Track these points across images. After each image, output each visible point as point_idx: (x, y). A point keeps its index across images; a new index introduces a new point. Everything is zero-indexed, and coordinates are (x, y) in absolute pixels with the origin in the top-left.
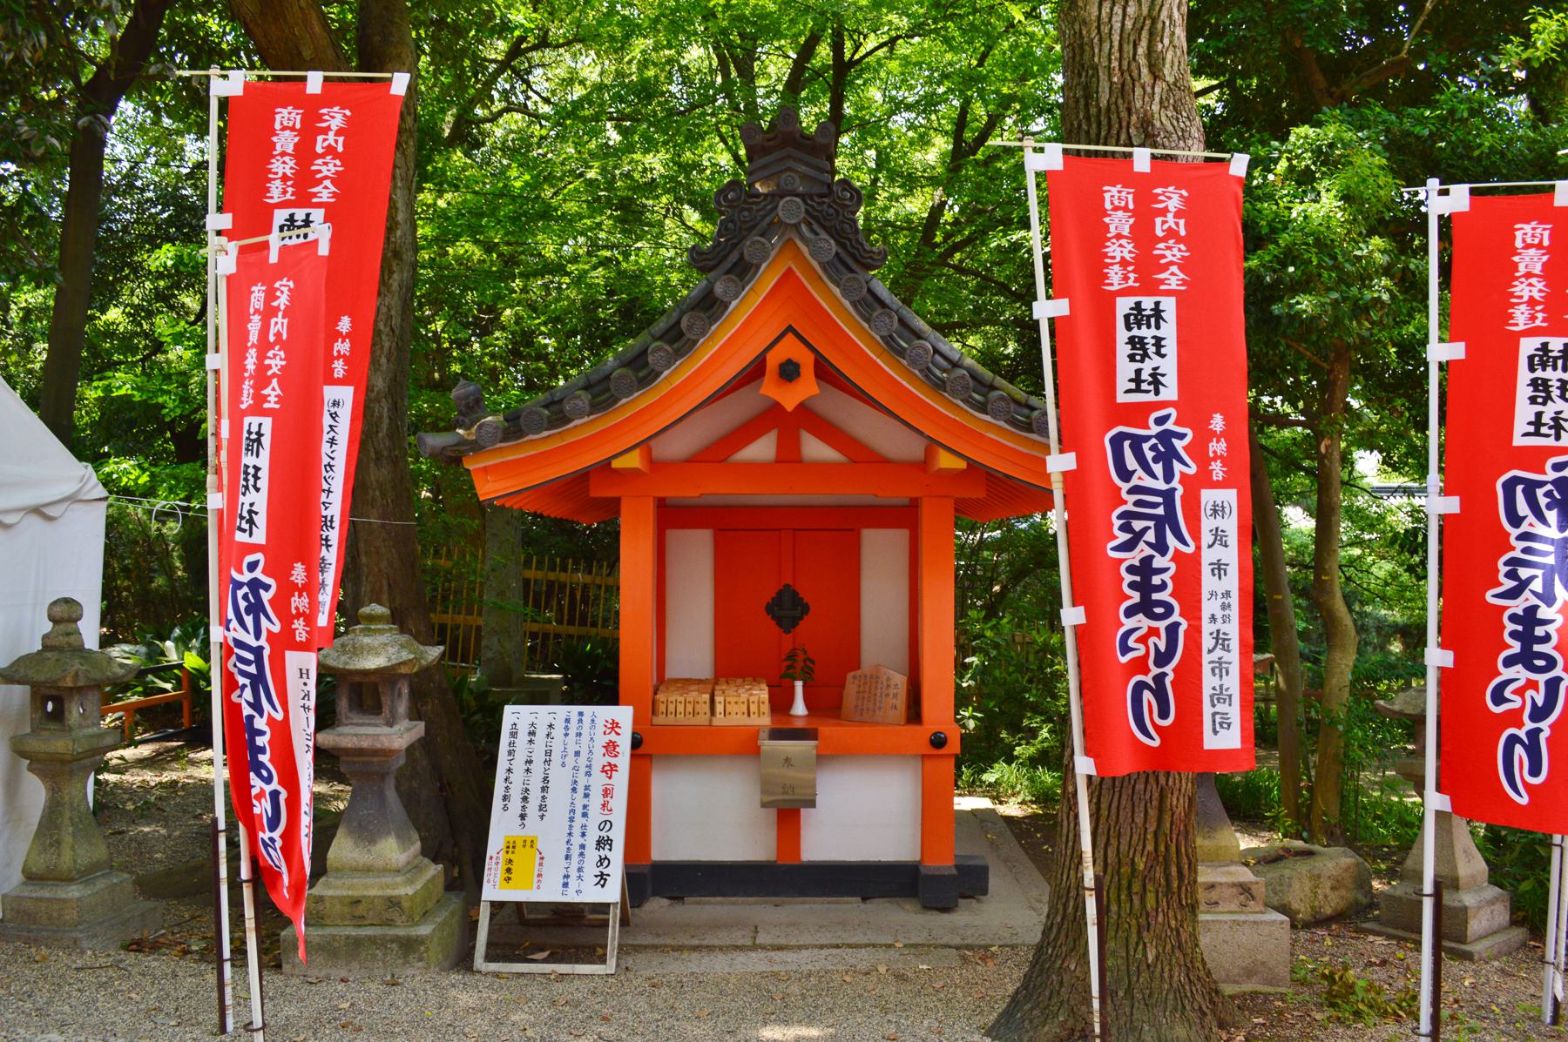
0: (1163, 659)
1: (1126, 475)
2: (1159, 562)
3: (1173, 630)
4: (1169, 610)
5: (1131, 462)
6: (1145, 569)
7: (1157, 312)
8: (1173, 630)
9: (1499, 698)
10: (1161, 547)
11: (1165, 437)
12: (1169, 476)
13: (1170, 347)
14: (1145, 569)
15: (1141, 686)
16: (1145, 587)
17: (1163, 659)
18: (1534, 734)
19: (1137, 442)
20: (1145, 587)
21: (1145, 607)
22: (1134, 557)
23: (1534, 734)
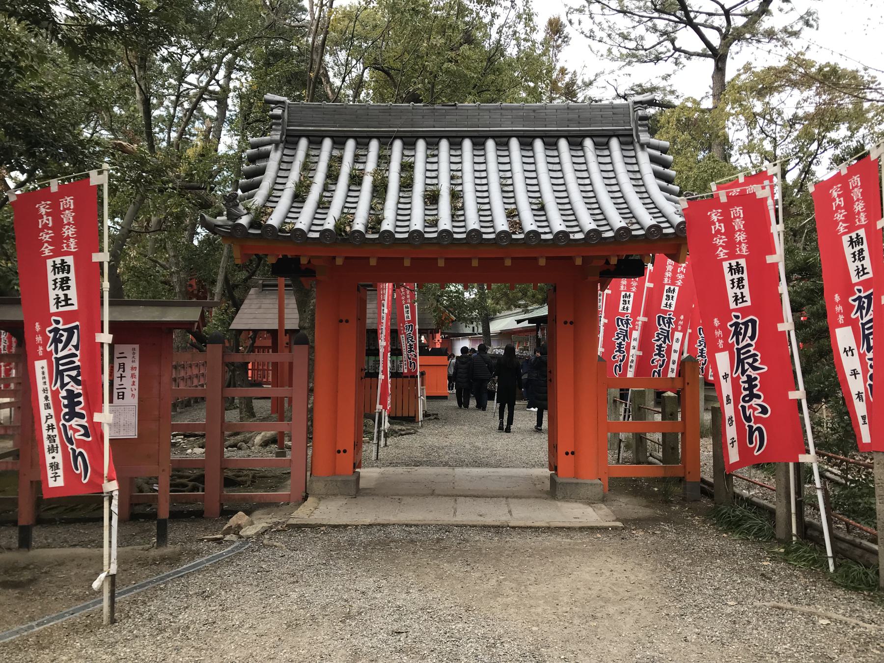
0: (621, 361)
1: (619, 326)
2: (623, 343)
3: (624, 356)
4: (624, 352)
5: (620, 324)
6: (620, 344)
7: (630, 295)
8: (624, 356)
9: (614, 358)
10: (624, 340)
11: (627, 320)
12: (627, 327)
13: (631, 303)
14: (620, 344)
15: (616, 366)
16: (620, 347)
17: (621, 361)
18: (620, 365)
19: (622, 320)
20: (620, 347)
21: (619, 351)
22: (618, 341)
23: (620, 365)
